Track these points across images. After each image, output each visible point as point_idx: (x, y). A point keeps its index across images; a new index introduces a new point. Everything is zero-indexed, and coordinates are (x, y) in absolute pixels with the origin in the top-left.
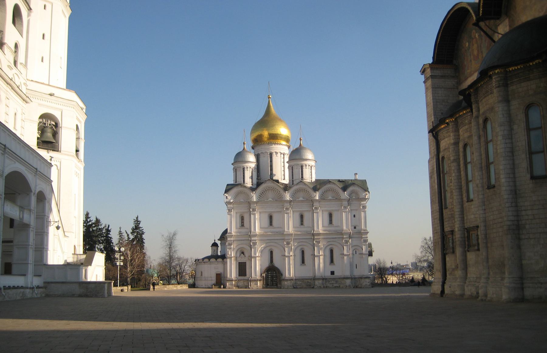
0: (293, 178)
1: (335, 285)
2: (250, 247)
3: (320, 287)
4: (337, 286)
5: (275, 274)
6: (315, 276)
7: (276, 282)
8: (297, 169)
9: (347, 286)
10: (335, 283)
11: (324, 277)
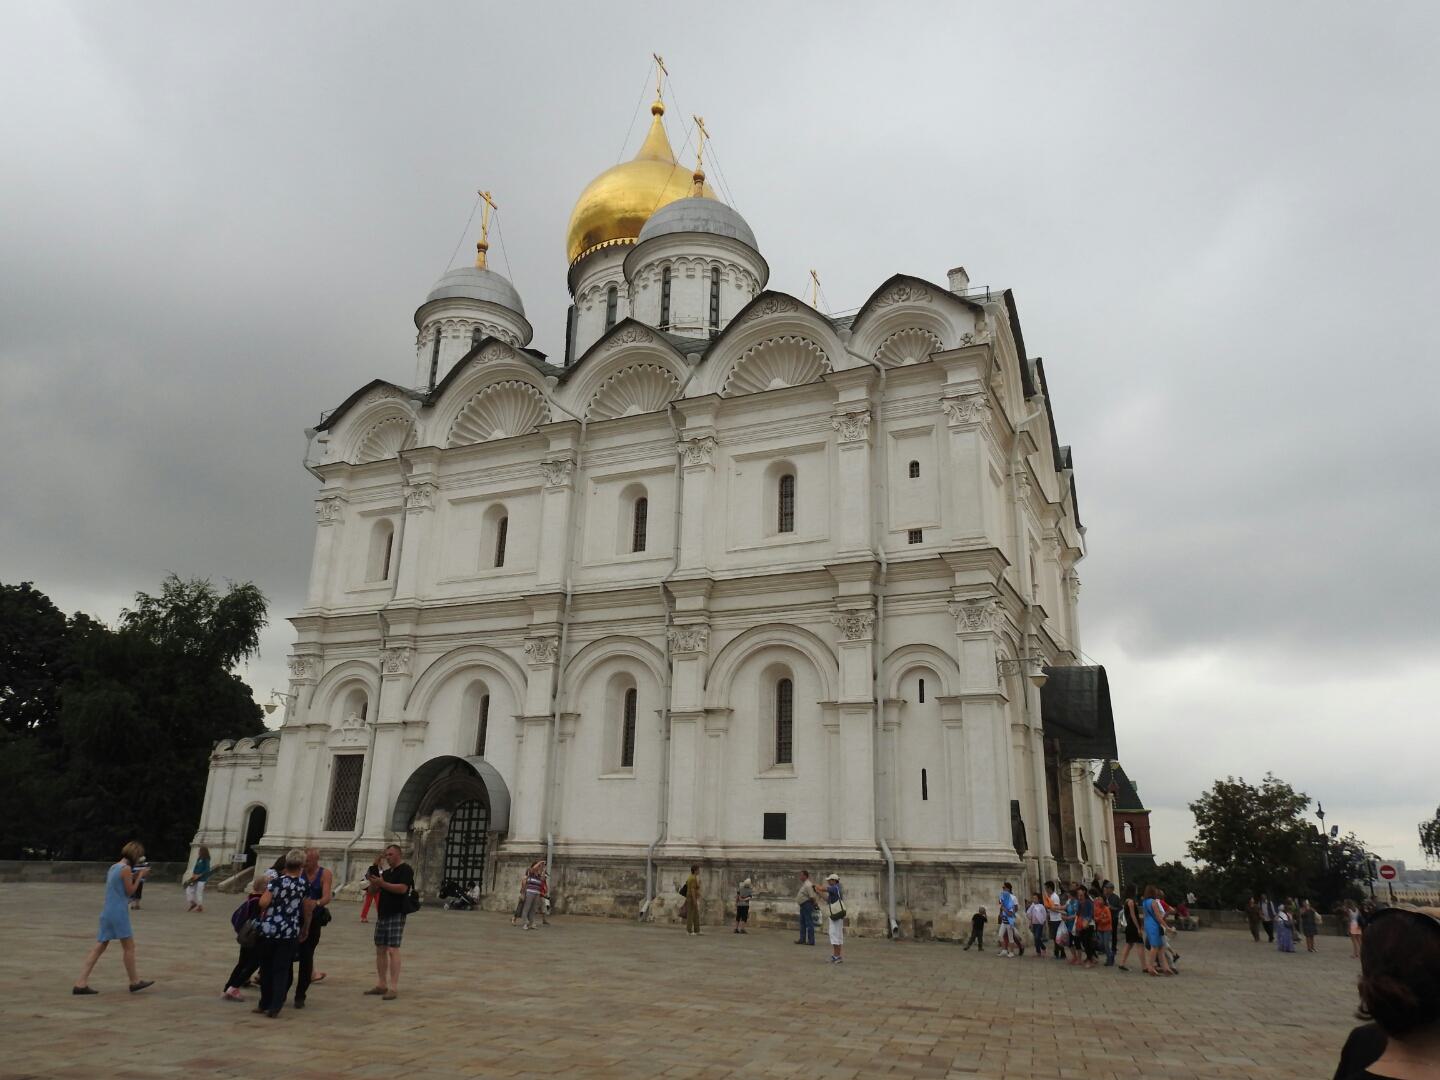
6: (661, 843)
10: (786, 892)
11: (715, 853)
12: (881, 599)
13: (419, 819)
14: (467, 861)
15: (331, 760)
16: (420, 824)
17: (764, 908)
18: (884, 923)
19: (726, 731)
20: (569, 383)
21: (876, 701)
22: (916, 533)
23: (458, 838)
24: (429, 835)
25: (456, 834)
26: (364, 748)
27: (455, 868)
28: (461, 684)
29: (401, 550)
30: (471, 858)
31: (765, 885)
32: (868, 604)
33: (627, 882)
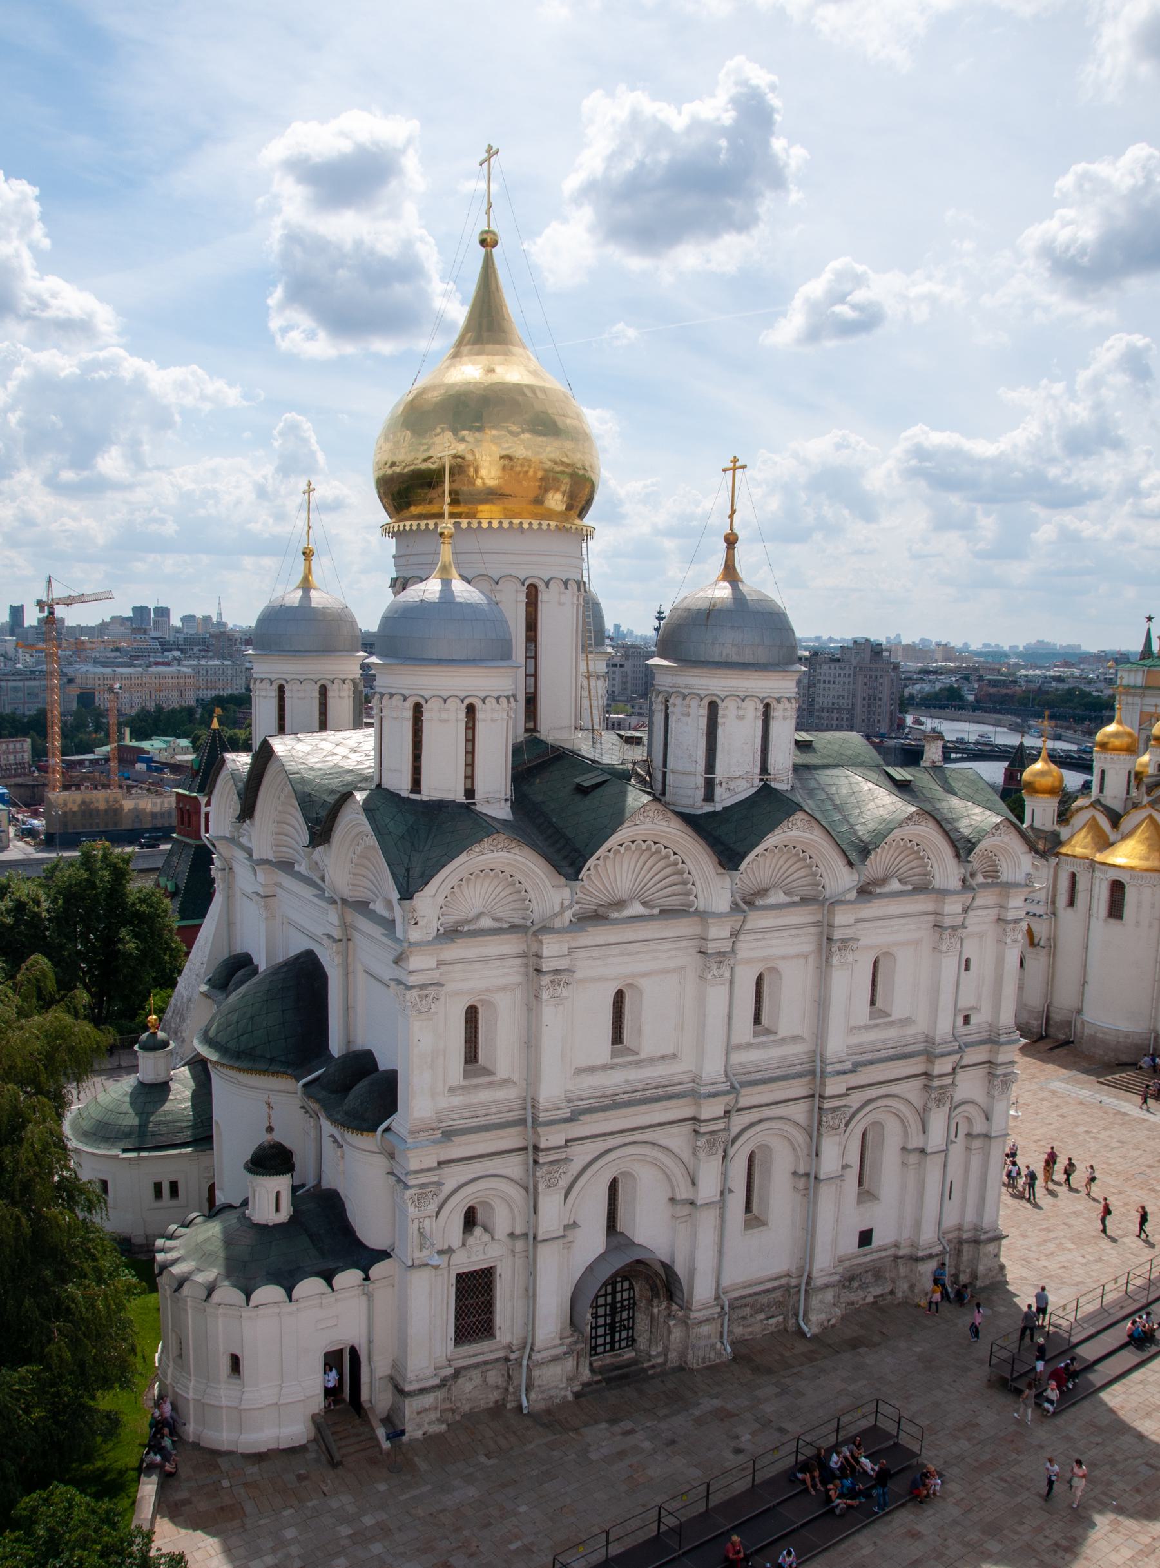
0: (710, 766)
2: (526, 1189)
5: (626, 1295)
8: (740, 718)
15: (453, 1281)
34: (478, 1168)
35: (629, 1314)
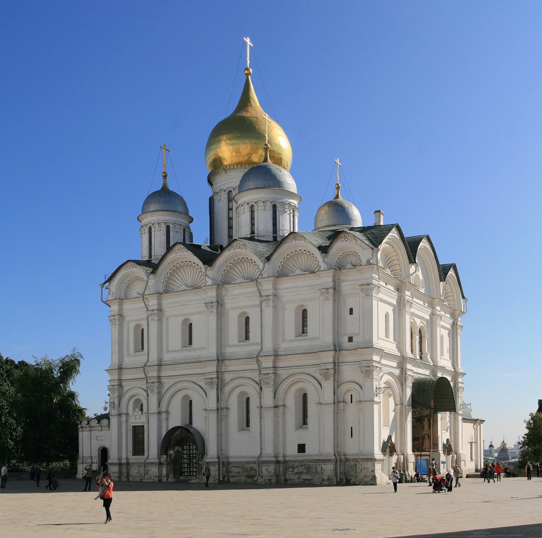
1: (304, 477)
3: (269, 480)
4: (308, 480)
7: (196, 468)
9: (323, 480)
10: (305, 471)
11: (281, 459)
12: (337, 364)
13: (170, 450)
14: (191, 465)
16: (171, 452)
17: (298, 477)
18: (335, 480)
19: (284, 414)
20: (213, 265)
21: (334, 403)
22: (351, 337)
23: (185, 456)
24: (174, 456)
25: (185, 455)
26: (144, 423)
27: (186, 468)
28: (180, 396)
29: (148, 339)
30: (191, 464)
31: (298, 470)
32: (332, 367)
33: (250, 470)
34: (134, 383)
35: (196, 461)
